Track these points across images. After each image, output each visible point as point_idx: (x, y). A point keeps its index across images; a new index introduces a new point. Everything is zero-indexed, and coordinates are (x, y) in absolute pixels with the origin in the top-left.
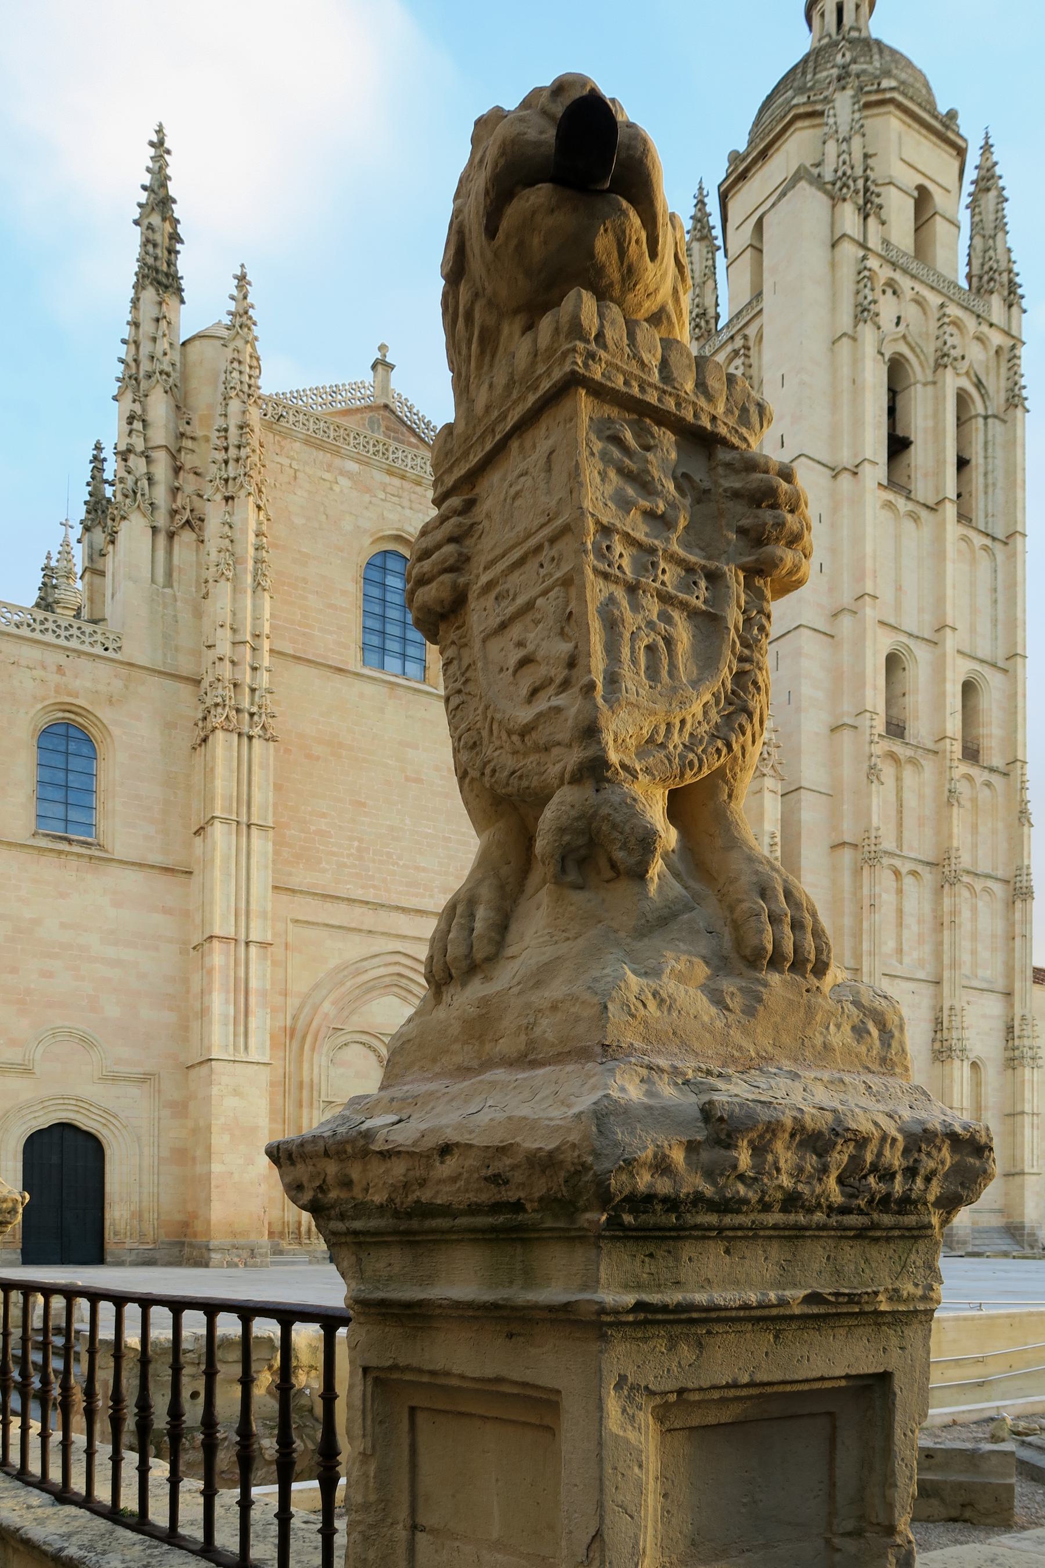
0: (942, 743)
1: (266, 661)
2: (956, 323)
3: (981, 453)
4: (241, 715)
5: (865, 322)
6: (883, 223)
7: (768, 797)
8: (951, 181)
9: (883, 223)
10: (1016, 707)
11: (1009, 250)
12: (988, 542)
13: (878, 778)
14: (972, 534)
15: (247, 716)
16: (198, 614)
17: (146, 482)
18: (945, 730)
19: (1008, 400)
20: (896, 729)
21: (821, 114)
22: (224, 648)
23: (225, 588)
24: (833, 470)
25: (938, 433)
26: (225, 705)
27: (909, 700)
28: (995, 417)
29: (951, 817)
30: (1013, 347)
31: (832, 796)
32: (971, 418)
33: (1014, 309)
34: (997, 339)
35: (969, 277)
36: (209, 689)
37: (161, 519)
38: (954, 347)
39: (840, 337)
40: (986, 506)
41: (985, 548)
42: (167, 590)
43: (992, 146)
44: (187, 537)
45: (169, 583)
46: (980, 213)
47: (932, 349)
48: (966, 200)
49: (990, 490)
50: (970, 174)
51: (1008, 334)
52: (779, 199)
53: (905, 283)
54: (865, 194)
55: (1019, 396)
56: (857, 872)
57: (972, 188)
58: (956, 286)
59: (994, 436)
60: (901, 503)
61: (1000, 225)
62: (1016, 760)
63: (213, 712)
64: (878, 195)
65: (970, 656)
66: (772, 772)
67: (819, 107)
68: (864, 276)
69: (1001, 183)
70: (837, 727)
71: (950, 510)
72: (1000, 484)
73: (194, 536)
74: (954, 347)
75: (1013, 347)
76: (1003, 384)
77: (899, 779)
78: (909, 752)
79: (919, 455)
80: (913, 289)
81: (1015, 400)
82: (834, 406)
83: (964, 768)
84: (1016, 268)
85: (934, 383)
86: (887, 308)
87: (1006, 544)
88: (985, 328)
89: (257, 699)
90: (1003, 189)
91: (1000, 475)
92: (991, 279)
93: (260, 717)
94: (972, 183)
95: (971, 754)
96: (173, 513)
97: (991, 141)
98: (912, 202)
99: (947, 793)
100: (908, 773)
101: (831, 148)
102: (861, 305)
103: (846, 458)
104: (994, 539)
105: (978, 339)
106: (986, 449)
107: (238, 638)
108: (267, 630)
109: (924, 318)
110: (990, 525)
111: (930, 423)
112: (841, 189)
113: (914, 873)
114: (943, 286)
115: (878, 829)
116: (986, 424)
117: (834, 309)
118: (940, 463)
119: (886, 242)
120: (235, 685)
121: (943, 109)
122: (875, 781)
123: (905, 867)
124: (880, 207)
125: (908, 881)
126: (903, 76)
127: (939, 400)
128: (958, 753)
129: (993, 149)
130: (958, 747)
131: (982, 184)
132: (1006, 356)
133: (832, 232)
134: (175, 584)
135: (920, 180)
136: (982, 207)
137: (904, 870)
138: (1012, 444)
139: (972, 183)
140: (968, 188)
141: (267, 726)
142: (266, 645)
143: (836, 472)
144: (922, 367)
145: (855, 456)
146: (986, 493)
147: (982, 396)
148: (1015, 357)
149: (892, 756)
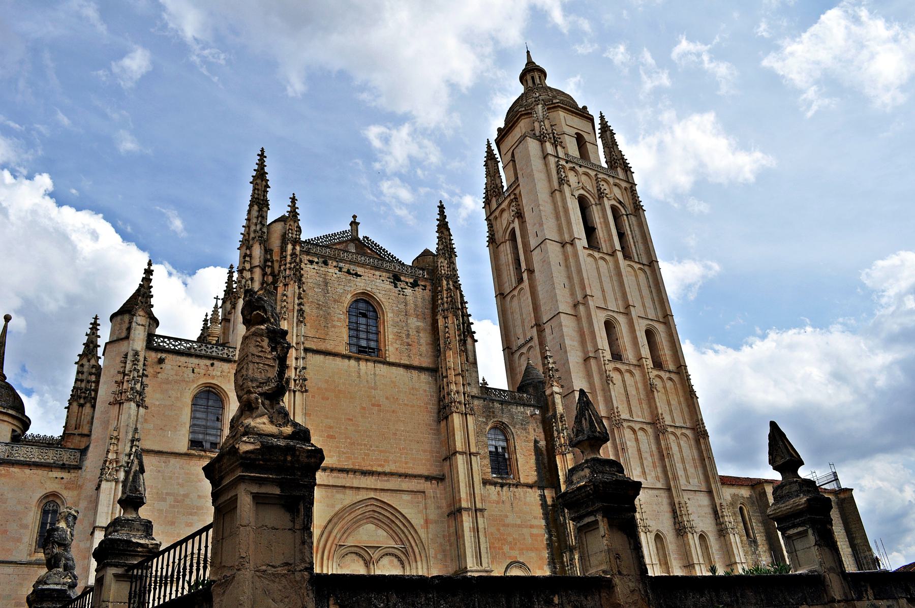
2: (605, 180)
6: (564, 148)
8: (590, 129)
10: (674, 339)
11: (621, 151)
12: (642, 266)
14: (632, 264)
17: (250, 282)
19: (634, 207)
21: (531, 113)
24: (562, 243)
27: (620, 341)
30: (632, 187)
32: (620, 216)
33: (628, 172)
34: (624, 185)
35: (606, 162)
38: (605, 190)
39: (554, 191)
40: (636, 251)
41: (640, 269)
48: (598, 135)
49: (636, 244)
51: (628, 182)
52: (519, 144)
54: (554, 138)
55: (640, 205)
57: (600, 131)
58: (601, 166)
60: (596, 254)
61: (615, 144)
62: (681, 365)
64: (559, 138)
67: (529, 111)
71: (620, 255)
74: (605, 190)
75: (632, 187)
76: (631, 201)
79: (601, 233)
81: (638, 208)
82: (558, 217)
84: (625, 157)
85: (600, 204)
88: (617, 181)
92: (615, 163)
101: (536, 124)
103: (567, 238)
104: (643, 265)
105: (615, 185)
106: (630, 228)
109: (589, 180)
111: (602, 220)
112: (543, 138)
116: (627, 218)
118: (610, 235)
119: (567, 154)
121: (580, 106)
124: (561, 142)
126: (562, 98)
127: (604, 210)
133: (543, 153)
140: (598, 131)
143: (563, 245)
144: (593, 199)
145: (571, 237)
146: (635, 246)
147: (623, 207)
148: (633, 190)
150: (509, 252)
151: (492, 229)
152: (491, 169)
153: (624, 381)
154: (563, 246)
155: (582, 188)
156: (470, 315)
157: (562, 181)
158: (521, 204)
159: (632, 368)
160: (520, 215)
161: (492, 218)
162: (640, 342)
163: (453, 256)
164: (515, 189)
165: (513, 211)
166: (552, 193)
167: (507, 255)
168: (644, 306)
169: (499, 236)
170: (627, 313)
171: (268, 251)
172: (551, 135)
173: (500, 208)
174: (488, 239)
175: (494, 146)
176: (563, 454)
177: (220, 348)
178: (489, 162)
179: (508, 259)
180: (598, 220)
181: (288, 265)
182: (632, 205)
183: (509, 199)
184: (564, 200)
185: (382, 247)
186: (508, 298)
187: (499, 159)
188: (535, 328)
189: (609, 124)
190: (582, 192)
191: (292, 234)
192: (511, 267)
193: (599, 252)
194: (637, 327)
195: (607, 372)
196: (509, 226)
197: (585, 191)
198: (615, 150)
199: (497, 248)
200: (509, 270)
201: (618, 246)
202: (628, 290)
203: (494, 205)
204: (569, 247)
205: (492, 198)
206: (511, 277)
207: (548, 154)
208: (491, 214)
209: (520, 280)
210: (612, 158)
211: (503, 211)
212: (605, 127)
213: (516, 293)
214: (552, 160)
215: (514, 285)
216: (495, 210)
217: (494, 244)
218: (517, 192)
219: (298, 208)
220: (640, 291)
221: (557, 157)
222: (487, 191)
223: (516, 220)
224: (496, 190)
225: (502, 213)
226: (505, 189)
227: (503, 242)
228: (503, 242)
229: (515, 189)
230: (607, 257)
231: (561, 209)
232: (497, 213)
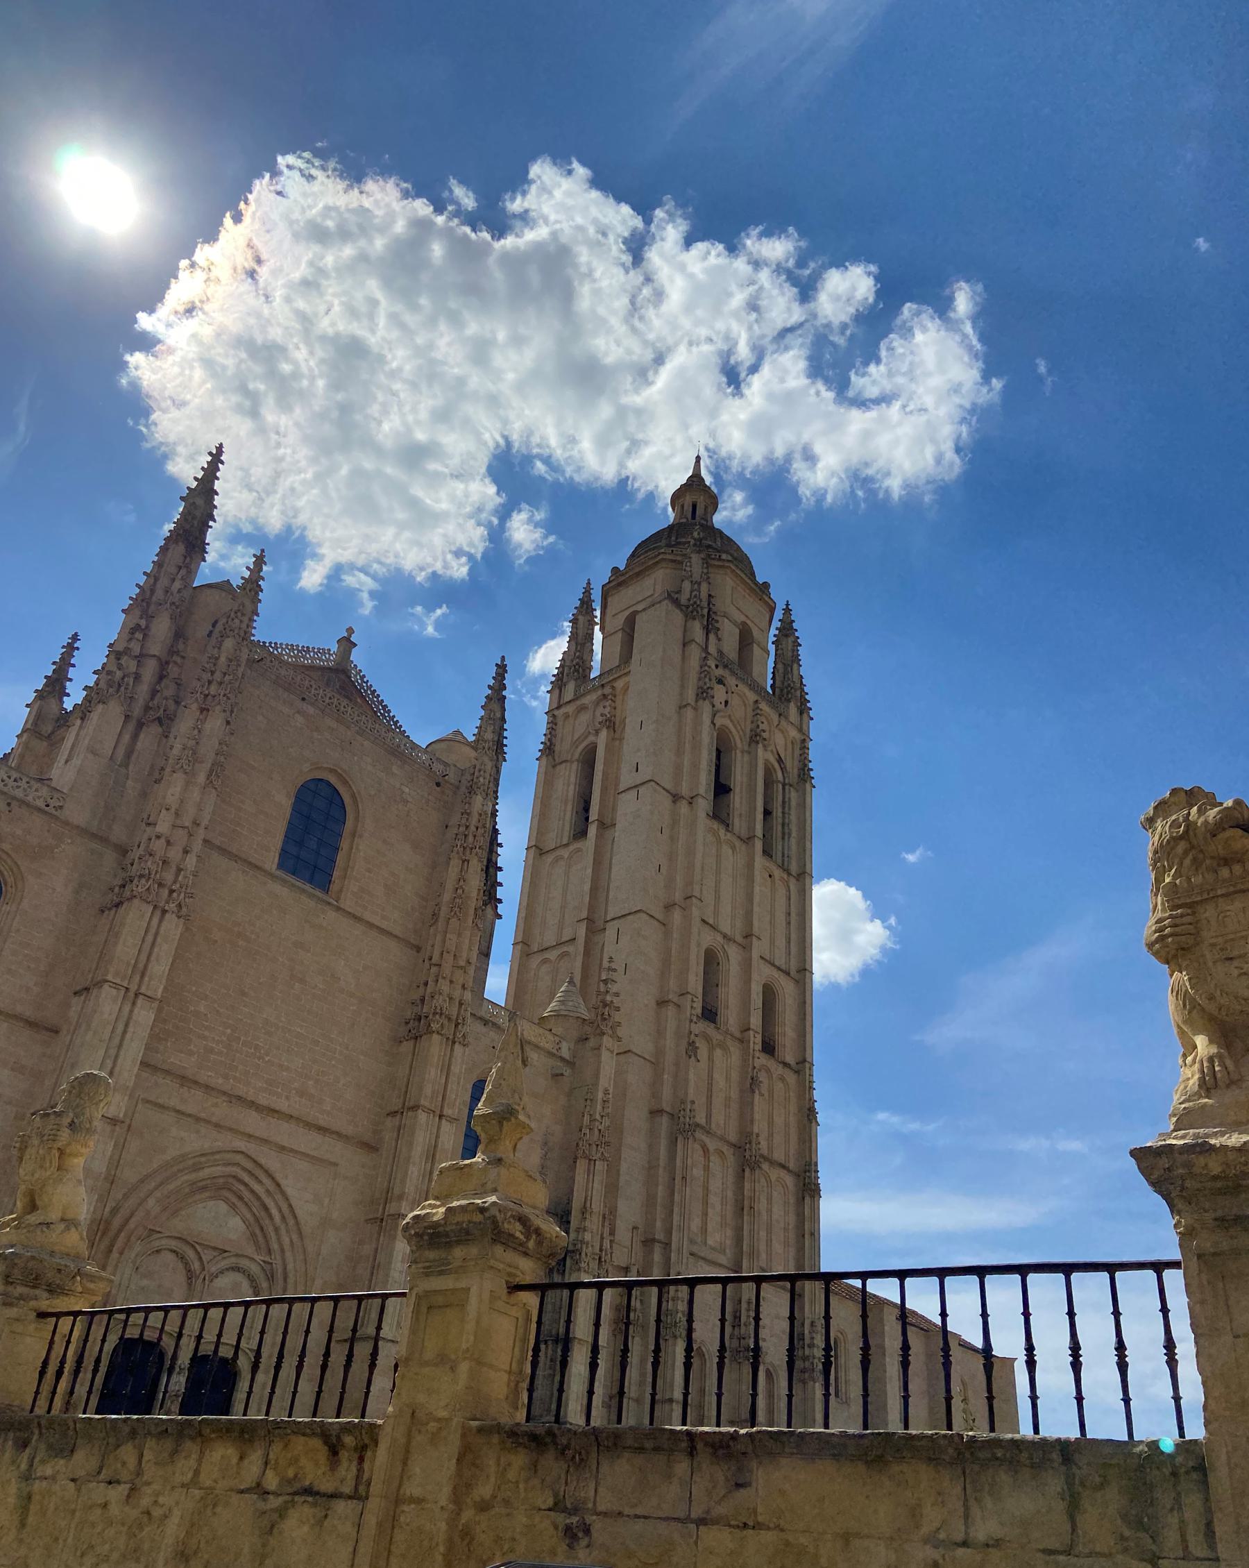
0: (746, 1033)
1: (197, 846)
3: (780, 810)
5: (705, 699)
6: (719, 640)
7: (605, 1056)
8: (764, 624)
9: (719, 640)
13: (696, 1056)
15: (167, 892)
16: (144, 795)
18: (749, 1023)
19: (799, 776)
20: (710, 1014)
22: (163, 827)
23: (179, 778)
25: (752, 789)
27: (722, 991)
28: (791, 785)
29: (752, 1103)
31: (656, 1064)
33: (805, 715)
34: (793, 733)
36: (136, 861)
37: (137, 711)
38: (764, 731)
39: (685, 706)
40: (783, 849)
41: (782, 879)
42: (123, 770)
44: (155, 729)
45: (126, 764)
47: (748, 731)
49: (786, 837)
50: (776, 624)
51: (800, 730)
53: (731, 681)
56: (673, 1142)
57: (777, 632)
59: (789, 799)
60: (722, 832)
61: (796, 659)
63: (135, 881)
65: (770, 963)
66: (610, 1032)
68: (704, 671)
70: (663, 1002)
71: (759, 845)
72: (794, 834)
73: (160, 730)
74: (764, 731)
75: (804, 741)
76: (796, 763)
77: (711, 1059)
78: (720, 1037)
79: (737, 799)
81: (804, 774)
82: (679, 752)
83: (762, 1060)
84: (806, 689)
85: (749, 753)
86: (719, 693)
87: (798, 880)
89: (180, 878)
91: (794, 829)
92: (788, 693)
93: (179, 895)
94: (777, 629)
95: (769, 1048)
96: (147, 708)
98: (737, 631)
99: (749, 1081)
100: (718, 1053)
102: (702, 688)
103: (685, 790)
104: (789, 874)
106: (784, 808)
107: (179, 822)
108: (205, 822)
110: (786, 863)
111: (745, 779)
114: (757, 688)
115: (693, 1102)
116: (784, 789)
118: (753, 809)
119: (720, 652)
120: (164, 862)
122: (693, 1058)
125: (714, 1159)
127: (753, 765)
128: (759, 1047)
130: (759, 1039)
132: (797, 747)
134: (131, 767)
135: (743, 618)
138: (804, 806)
139: (777, 629)
141: (183, 905)
142: (201, 833)
143: (676, 798)
146: (783, 838)
149: (708, 1039)
150: (573, 779)
151: (553, 732)
152: (581, 632)
153: (711, 1059)
154: (674, 802)
155: (730, 716)
156: (500, 869)
157: (703, 693)
159: (729, 1042)
160: (611, 724)
161: (558, 713)
162: (752, 1002)
163: (500, 757)
164: (615, 679)
166: (680, 708)
167: (569, 785)
168: (772, 942)
169: (562, 748)
170: (746, 948)
171: (179, 635)
172: (705, 611)
173: (578, 703)
174: (541, 747)
175: (596, 595)
176: (592, 1161)
177: (36, 785)
178: (580, 617)
179: (567, 791)
180: (738, 778)
181: (218, 676)
182: (796, 771)
185: (382, 701)
186: (549, 858)
187: (598, 620)
188: (584, 926)
190: (727, 722)
191: (241, 621)
192: (569, 807)
193: (727, 830)
194: (755, 976)
195: (692, 1036)
196: (586, 737)
197: (731, 721)
198: (795, 672)
199: (554, 766)
200: (565, 811)
201: (759, 832)
202: (756, 909)
204: (683, 808)
205: (568, 682)
206: (563, 825)
207: (693, 640)
208: (558, 708)
209: (581, 833)
210: (786, 684)
211: (583, 708)
212: (787, 629)
213: (565, 853)
214: (695, 654)
215: (565, 841)
216: (570, 702)
217: (550, 757)
218: (619, 684)
219: (263, 579)
220: (772, 914)
221: (706, 650)
223: (604, 734)
225: (579, 712)
227: (566, 761)
228: (566, 761)
229: (615, 679)
230: (738, 843)
232: (569, 709)
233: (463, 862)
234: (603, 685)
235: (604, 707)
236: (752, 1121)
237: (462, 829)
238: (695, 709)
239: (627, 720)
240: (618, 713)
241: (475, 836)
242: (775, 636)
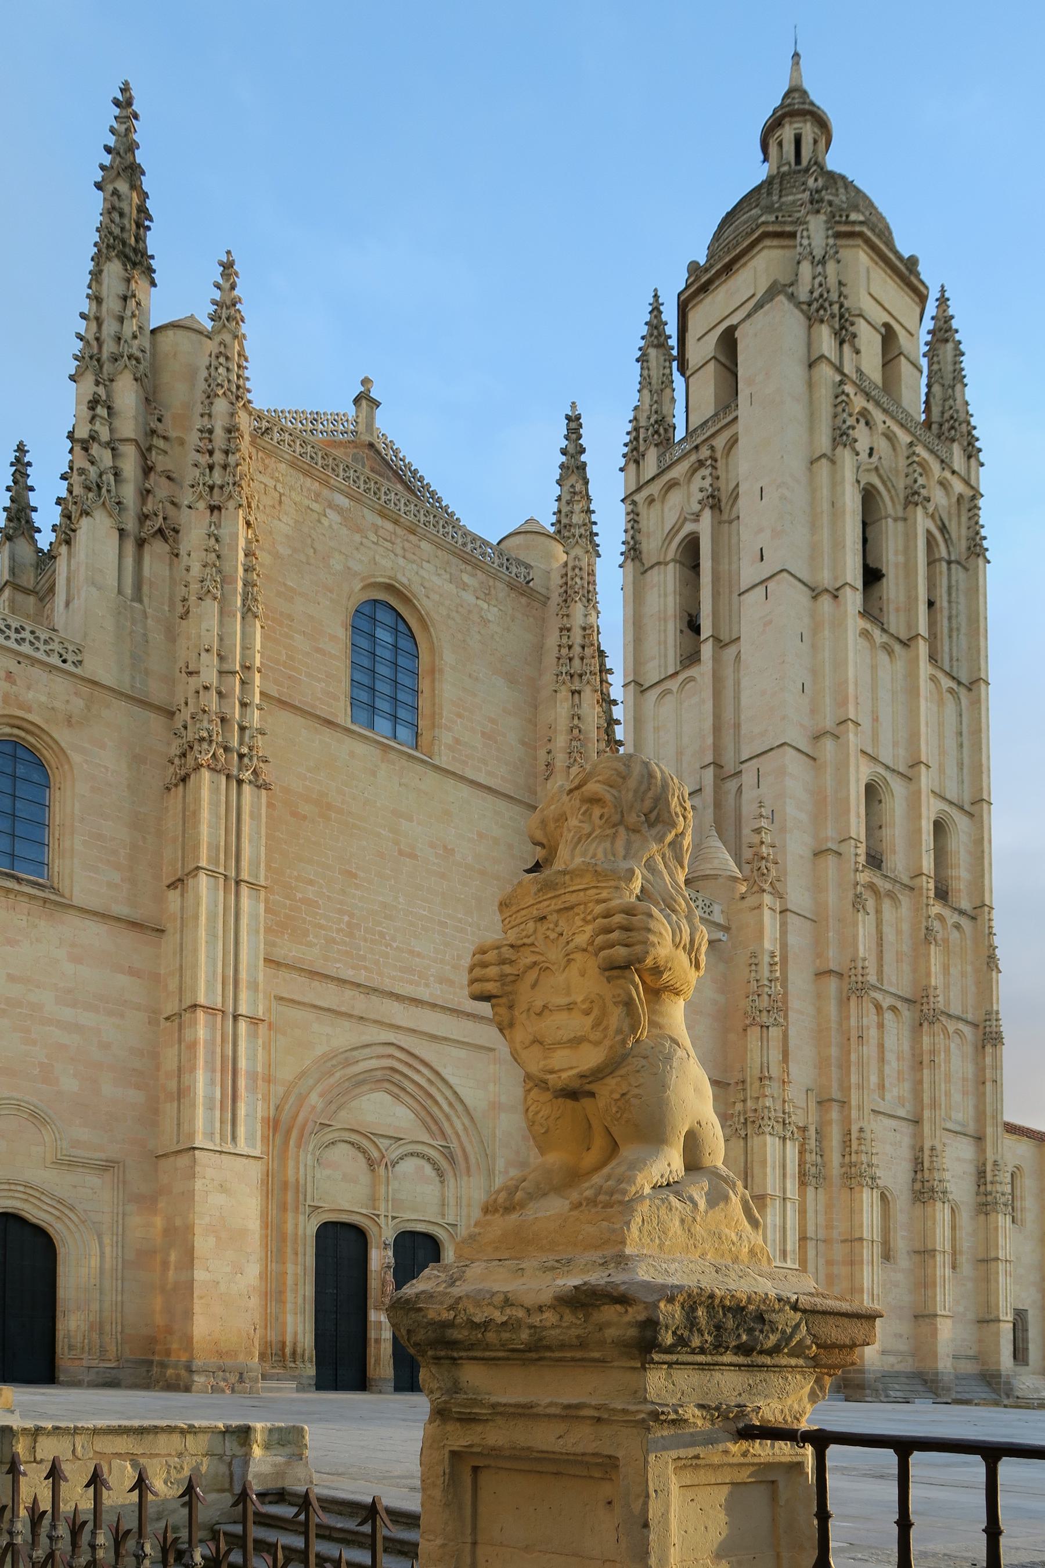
4: (229, 755)
26: (211, 741)
39: (820, 457)
43: (948, 300)
46: (939, 363)
50: (928, 324)
57: (929, 338)
69: (957, 337)
80: (884, 422)
86: (862, 436)
89: (247, 739)
90: (960, 342)
93: (251, 759)
94: (929, 332)
97: (947, 295)
113: (893, 1009)
117: (812, 429)
123: (886, 1002)
129: (949, 303)
131: (939, 335)
136: (941, 357)
137: (885, 1005)
139: (929, 332)
157: (842, 437)
158: (723, 476)
165: (701, 490)
166: (812, 463)
173: (666, 478)
183: (693, 458)
184: (835, 484)
189: (955, 324)
203: (650, 465)
211: (672, 485)
216: (653, 479)
218: (720, 442)
222: (636, 429)
224: (662, 431)
226: (680, 434)
231: (825, 506)
233: (573, 693)
234: (697, 447)
235: (703, 478)
236: (928, 974)
237: (564, 651)
238: (833, 462)
239: (741, 490)
240: (722, 484)
241: (582, 659)
242: (927, 344)
